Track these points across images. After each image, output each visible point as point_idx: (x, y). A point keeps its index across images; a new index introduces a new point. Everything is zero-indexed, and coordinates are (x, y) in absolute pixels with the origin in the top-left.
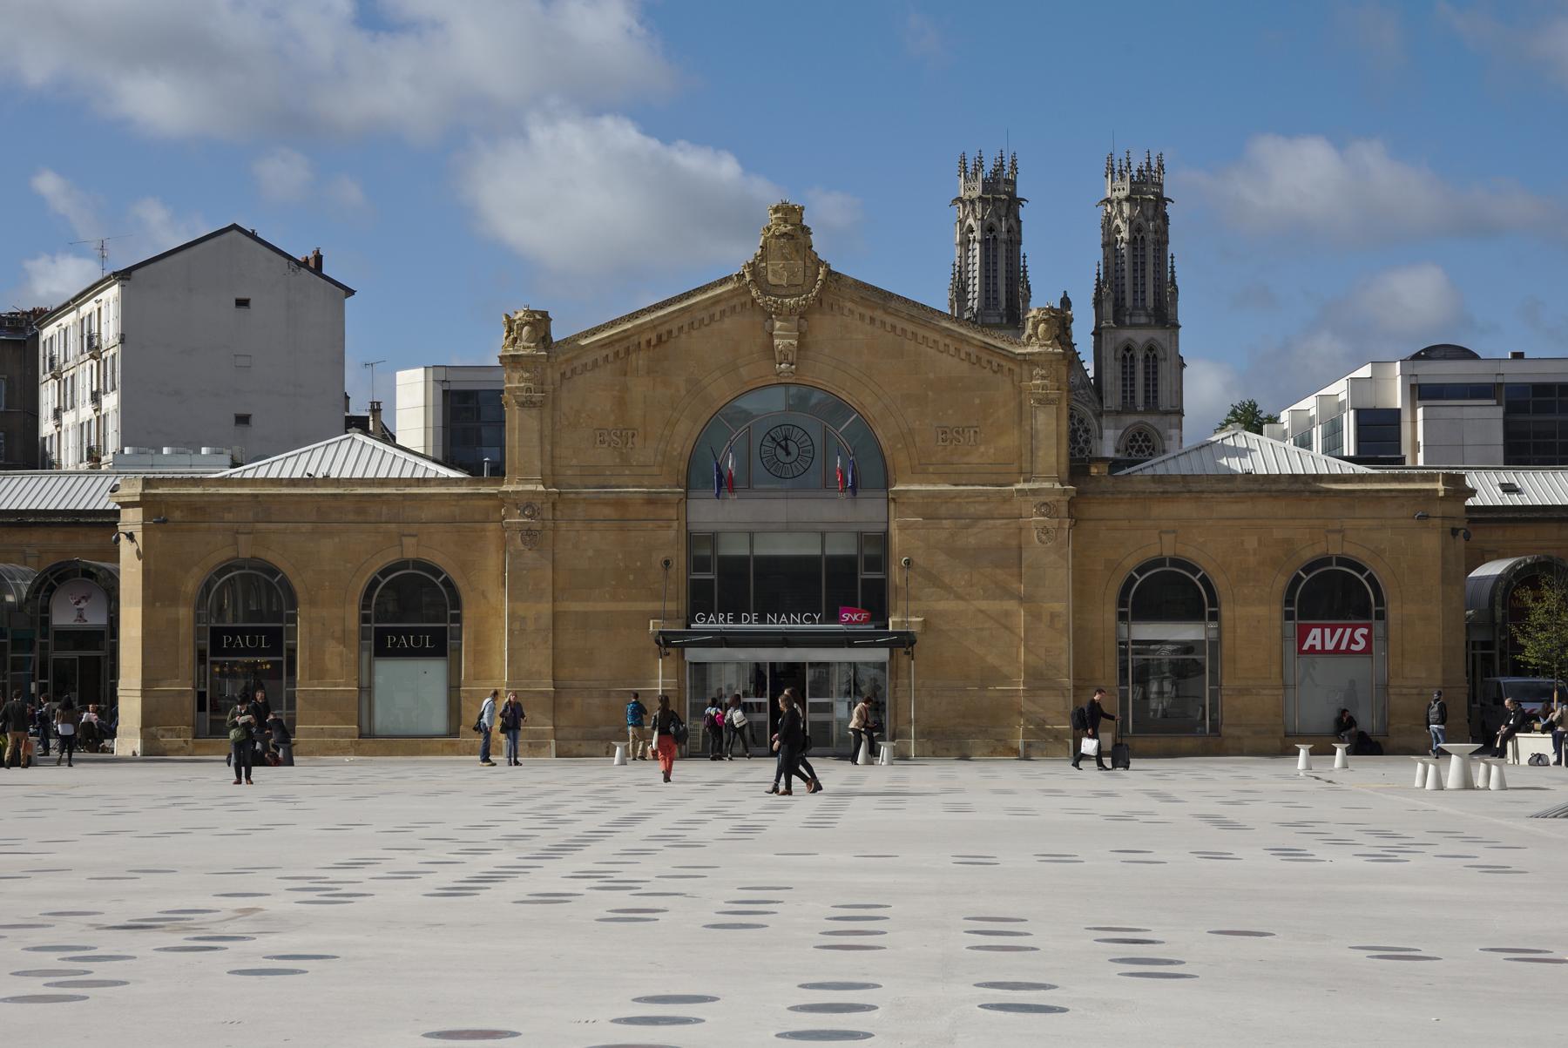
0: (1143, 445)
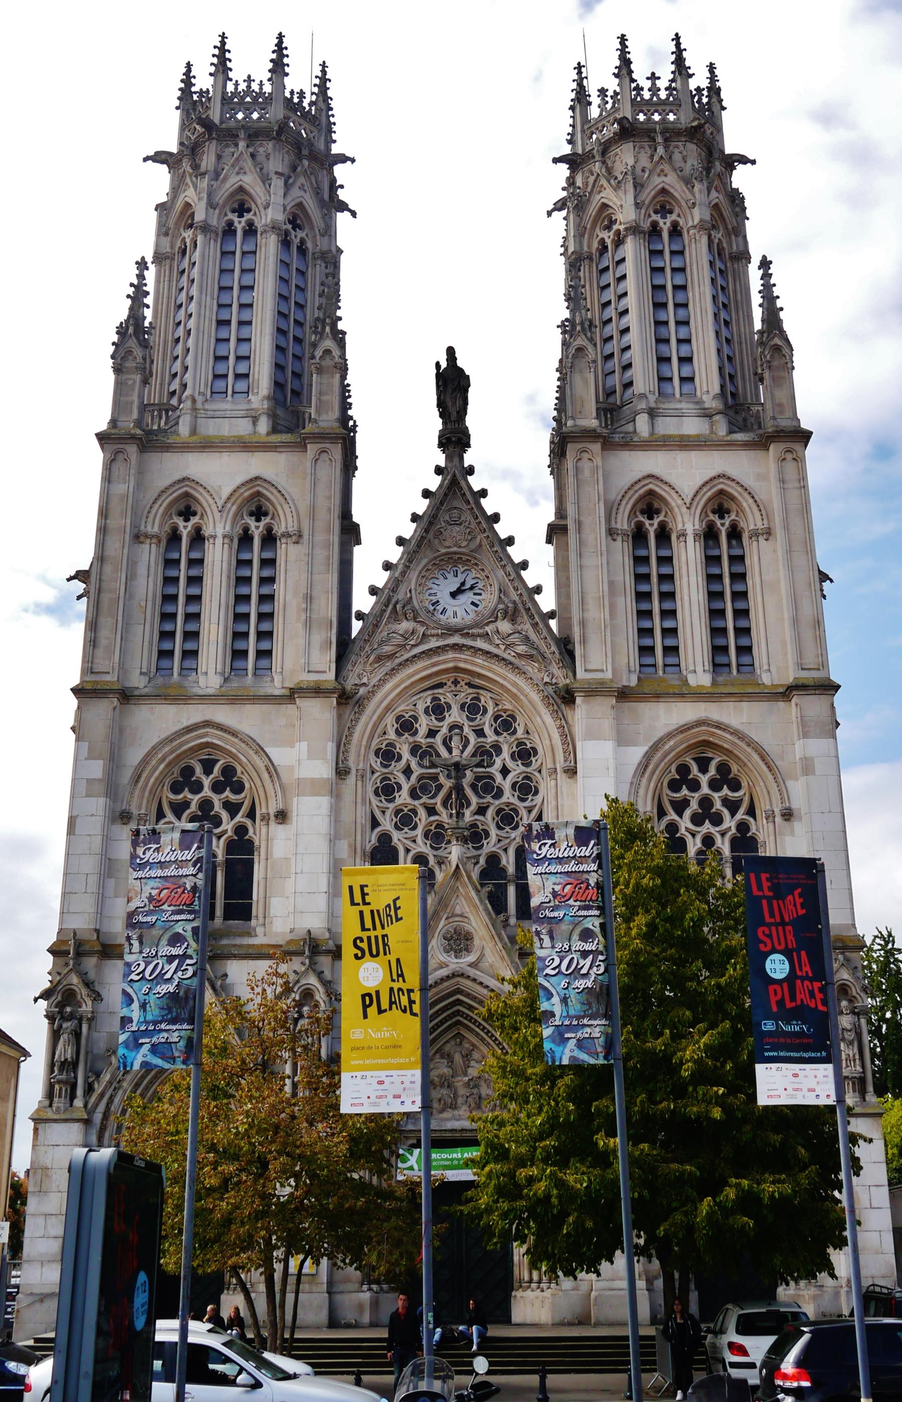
0: (716, 796)
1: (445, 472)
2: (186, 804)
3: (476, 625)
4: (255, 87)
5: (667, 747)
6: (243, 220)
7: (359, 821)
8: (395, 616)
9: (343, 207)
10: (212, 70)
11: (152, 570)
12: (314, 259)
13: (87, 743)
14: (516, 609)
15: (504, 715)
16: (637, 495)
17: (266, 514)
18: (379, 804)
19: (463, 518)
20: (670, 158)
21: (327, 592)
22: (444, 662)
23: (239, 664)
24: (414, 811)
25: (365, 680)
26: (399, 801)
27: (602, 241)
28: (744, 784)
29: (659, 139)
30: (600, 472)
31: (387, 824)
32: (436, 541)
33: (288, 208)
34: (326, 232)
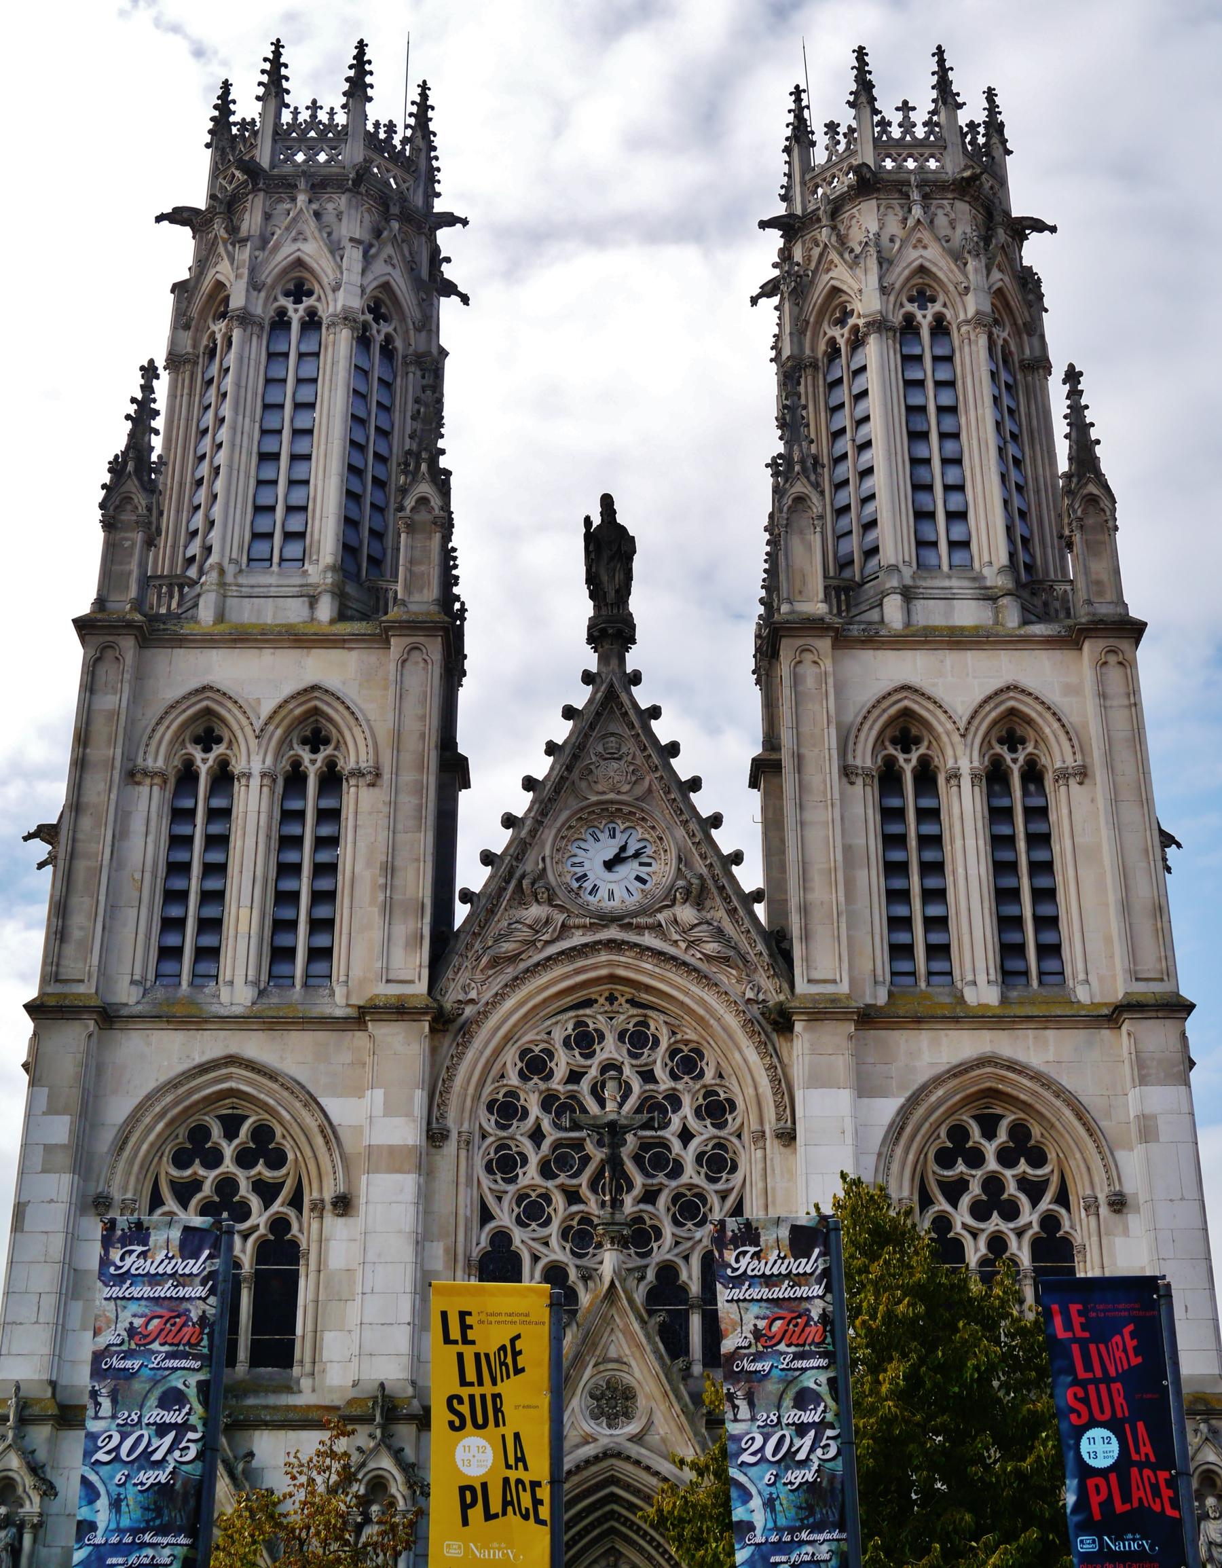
1: (598, 680)
2: (196, 1185)
3: (643, 911)
4: (323, 116)
5: (933, 1098)
6: (301, 307)
7: (461, 1211)
8: (520, 898)
9: (450, 289)
10: (261, 91)
11: (153, 824)
12: (405, 364)
13: (46, 1090)
14: (703, 887)
15: (685, 1049)
16: (885, 717)
17: (327, 742)
18: (493, 1186)
19: (624, 750)
20: (932, 222)
21: (418, 860)
22: (595, 967)
23: (282, 969)
24: (547, 1197)
25: (473, 995)
26: (523, 1181)
27: (832, 342)
28: (1052, 1156)
29: (915, 195)
30: (831, 681)
31: (505, 1217)
32: (584, 785)
33: (368, 291)
34: (424, 326)
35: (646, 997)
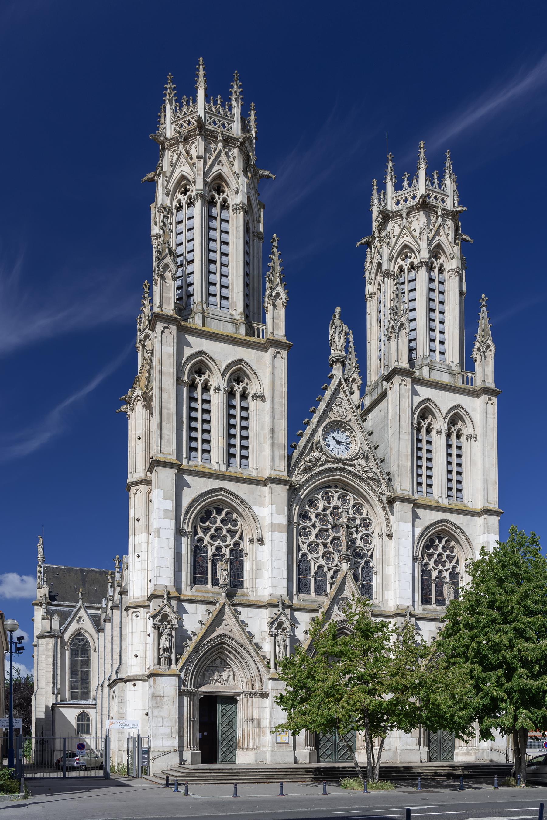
3: (351, 460)
35: (346, 488)
